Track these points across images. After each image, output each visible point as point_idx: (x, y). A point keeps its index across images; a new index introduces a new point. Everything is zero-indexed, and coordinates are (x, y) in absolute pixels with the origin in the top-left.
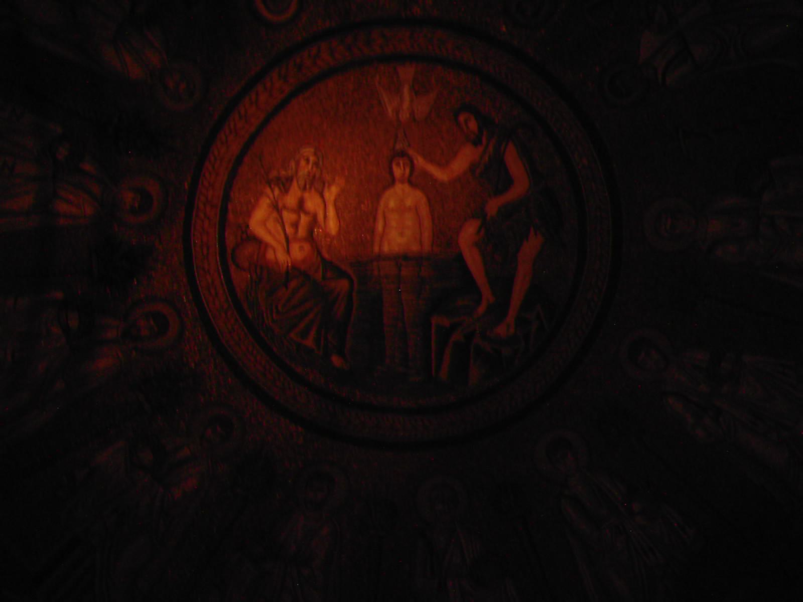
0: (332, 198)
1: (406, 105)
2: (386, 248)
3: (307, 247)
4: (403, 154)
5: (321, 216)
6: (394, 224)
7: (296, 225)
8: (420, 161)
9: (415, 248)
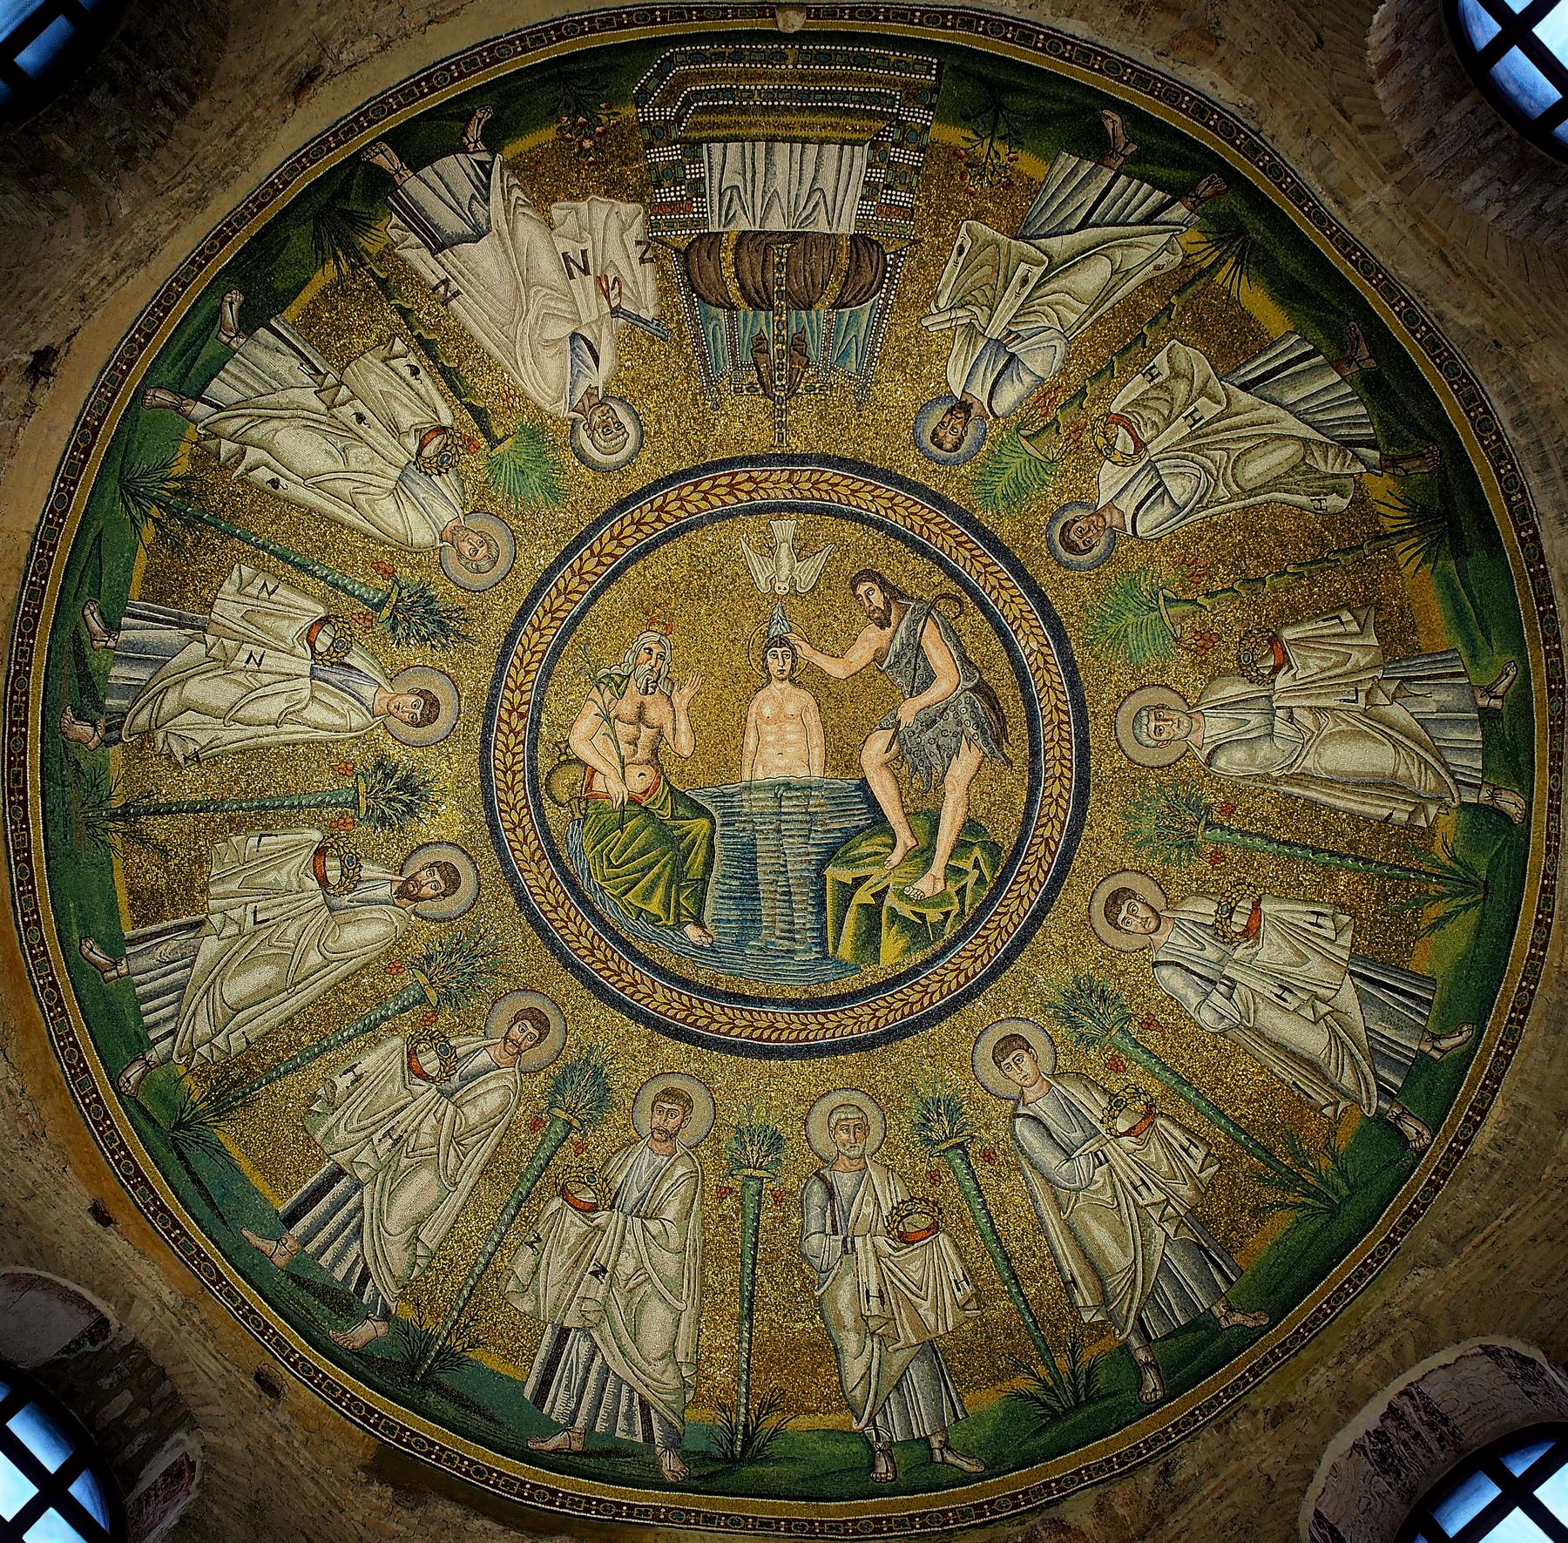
0: (684, 705)
1: (785, 571)
2: (760, 775)
3: (649, 771)
4: (782, 641)
5: (668, 730)
6: (770, 738)
7: (634, 742)
8: (804, 650)
9: (802, 773)
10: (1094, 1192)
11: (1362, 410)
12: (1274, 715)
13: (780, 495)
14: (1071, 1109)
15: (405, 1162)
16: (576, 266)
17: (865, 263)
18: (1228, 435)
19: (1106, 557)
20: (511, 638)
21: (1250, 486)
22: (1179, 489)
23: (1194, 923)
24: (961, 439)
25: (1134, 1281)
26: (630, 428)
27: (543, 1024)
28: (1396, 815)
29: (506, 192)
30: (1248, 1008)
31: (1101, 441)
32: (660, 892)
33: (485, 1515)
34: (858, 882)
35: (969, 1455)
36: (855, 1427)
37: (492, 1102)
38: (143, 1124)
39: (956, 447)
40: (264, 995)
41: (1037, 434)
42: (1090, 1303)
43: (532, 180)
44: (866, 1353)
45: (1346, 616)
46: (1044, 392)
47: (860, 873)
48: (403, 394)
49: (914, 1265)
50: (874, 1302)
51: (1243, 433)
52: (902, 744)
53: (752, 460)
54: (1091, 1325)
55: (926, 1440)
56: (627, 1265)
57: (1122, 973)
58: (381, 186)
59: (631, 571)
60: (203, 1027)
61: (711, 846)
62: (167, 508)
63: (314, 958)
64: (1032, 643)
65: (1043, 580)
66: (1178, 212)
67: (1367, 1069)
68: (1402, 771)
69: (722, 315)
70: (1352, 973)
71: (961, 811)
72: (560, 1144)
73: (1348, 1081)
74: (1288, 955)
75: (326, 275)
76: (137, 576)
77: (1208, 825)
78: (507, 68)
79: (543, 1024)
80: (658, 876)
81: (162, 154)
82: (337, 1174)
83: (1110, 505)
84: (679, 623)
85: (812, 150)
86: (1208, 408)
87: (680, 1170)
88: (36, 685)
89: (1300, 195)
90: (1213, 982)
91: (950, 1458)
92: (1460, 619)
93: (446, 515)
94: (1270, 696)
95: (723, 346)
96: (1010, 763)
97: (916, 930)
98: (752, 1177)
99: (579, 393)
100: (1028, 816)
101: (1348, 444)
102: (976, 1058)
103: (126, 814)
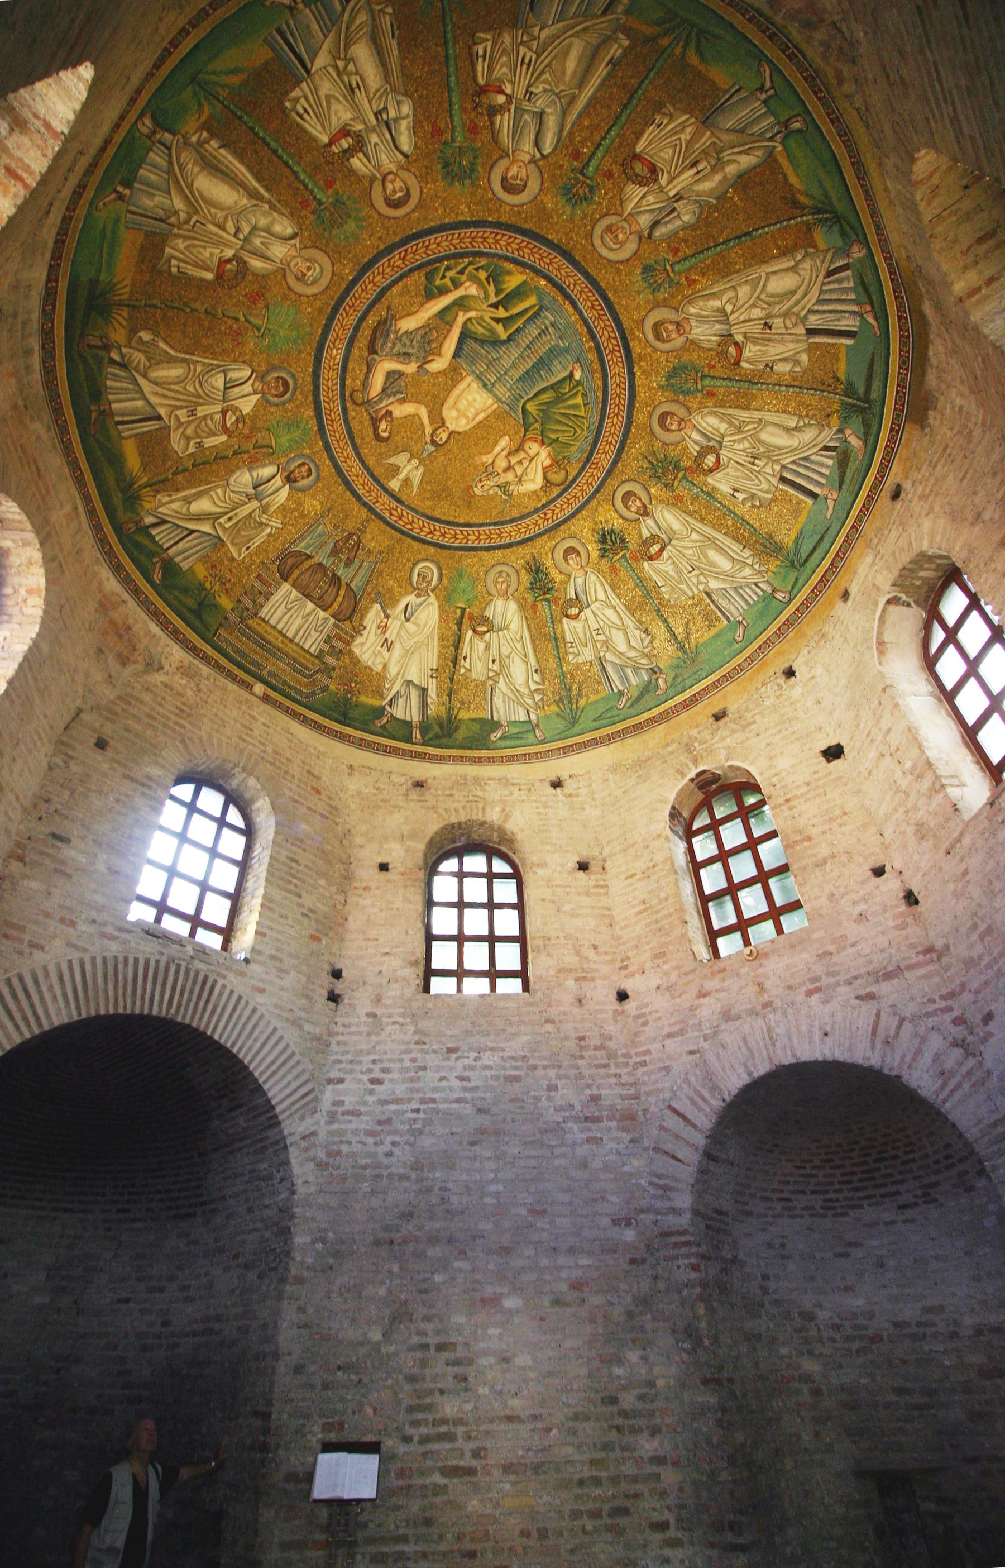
1: (409, 467)
2: (490, 401)
3: (526, 447)
4: (433, 442)
5: (505, 453)
6: (473, 410)
7: (520, 462)
8: (428, 430)
9: (474, 385)
10: (549, 84)
11: (109, 383)
12: (245, 238)
13: (386, 498)
14: (517, 131)
15: (762, 450)
16: (388, 645)
17: (288, 568)
18: (181, 397)
19: (273, 368)
20: (521, 543)
21: (184, 365)
22: (219, 381)
23: (369, 160)
24: (300, 466)
25: (584, 30)
26: (416, 571)
27: (664, 416)
28: (216, 146)
29: (389, 689)
30: (381, 97)
31: (240, 426)
32: (571, 402)
33: (926, 355)
34: (498, 320)
35: (760, 73)
36: (780, 148)
37: (712, 420)
38: (799, 585)
39: (303, 464)
40: (721, 550)
41: (267, 447)
42: (616, 46)
43: (378, 687)
44: (733, 157)
45: (174, 270)
46: (253, 463)
47: (494, 324)
48: (475, 655)
49: (665, 158)
50: (701, 167)
51: (173, 394)
52: (424, 358)
53: (387, 523)
54: (628, 38)
55: (764, 102)
56: (756, 313)
57: (427, 167)
58: (425, 727)
59: (461, 521)
60: (747, 572)
61: (536, 395)
62: (570, 702)
63: (695, 536)
64: (335, 354)
65: (309, 379)
66: (149, 520)
67: (346, 15)
68: (197, 169)
69: (353, 585)
70: (308, 72)
71: (427, 306)
72: (714, 377)
73: (363, 17)
74: (335, 106)
75: (463, 715)
76: (599, 696)
77: (320, 203)
78: (359, 734)
79: (664, 416)
80: (565, 408)
81: (475, 817)
82: (783, 480)
83: (255, 393)
84: (463, 486)
85: (280, 627)
86: (182, 415)
87: (692, 310)
88: (656, 711)
89: (91, 513)
90: (387, 123)
91: (768, 84)
92: (114, 244)
93: (499, 603)
94: (242, 248)
95: (362, 572)
96: (389, 308)
97: (495, 277)
98: (673, 271)
99: (422, 599)
100: (401, 278)
101: (123, 366)
102: (531, 198)
103: (682, 648)
